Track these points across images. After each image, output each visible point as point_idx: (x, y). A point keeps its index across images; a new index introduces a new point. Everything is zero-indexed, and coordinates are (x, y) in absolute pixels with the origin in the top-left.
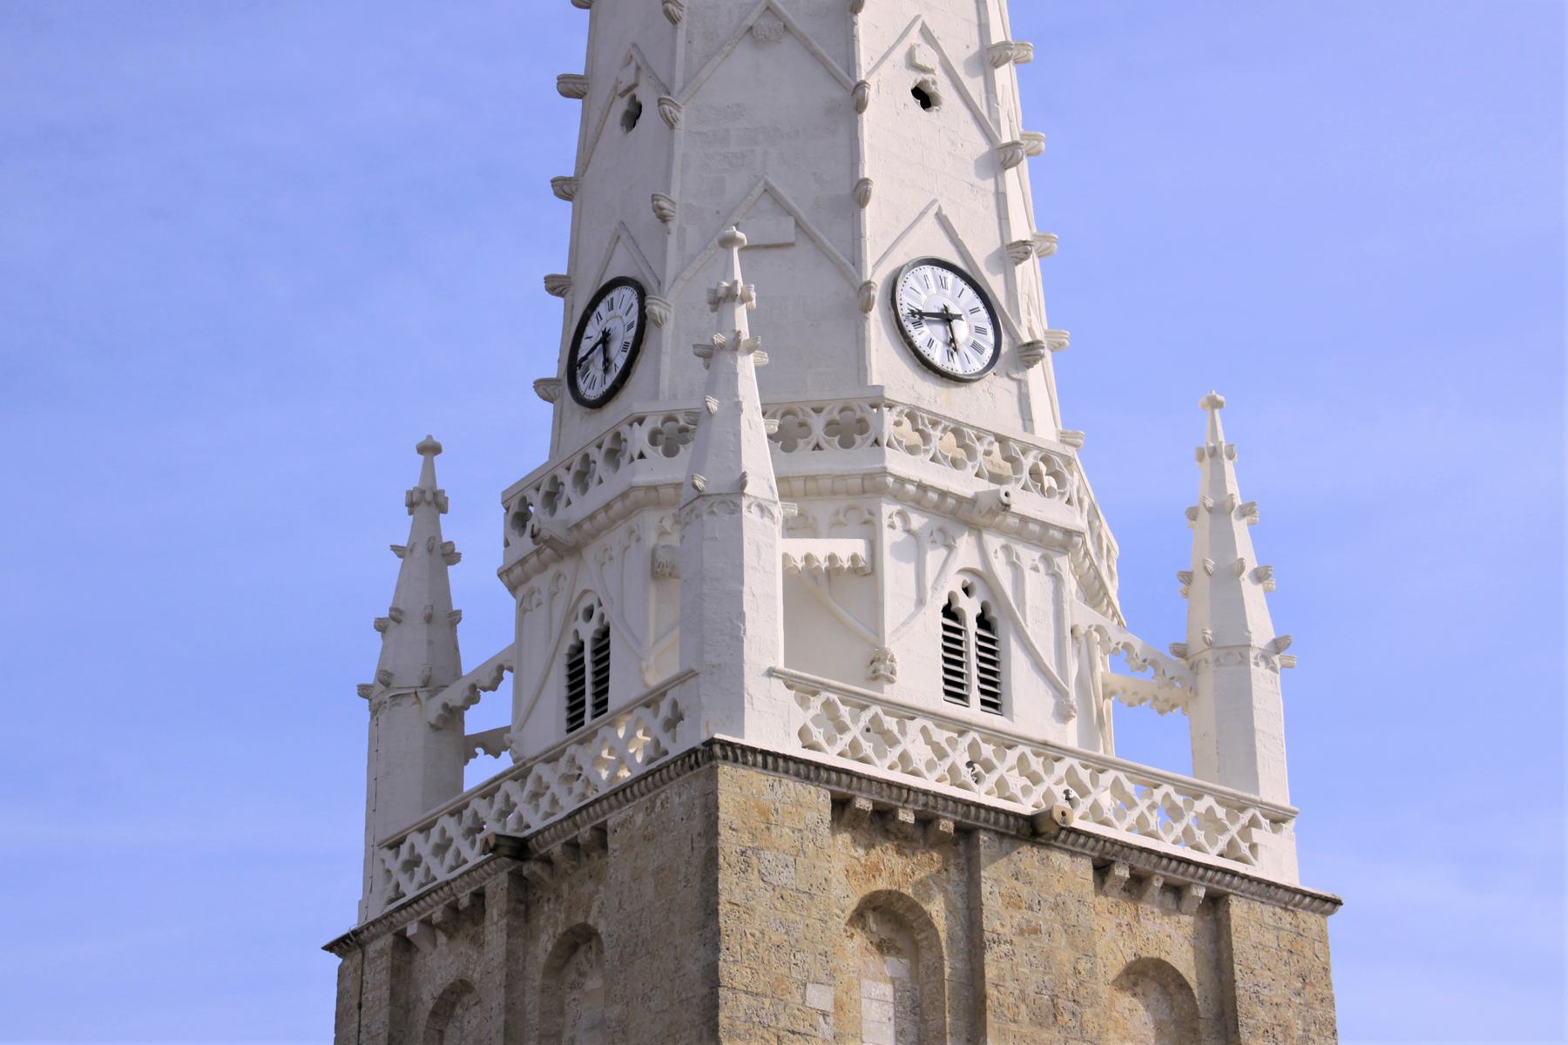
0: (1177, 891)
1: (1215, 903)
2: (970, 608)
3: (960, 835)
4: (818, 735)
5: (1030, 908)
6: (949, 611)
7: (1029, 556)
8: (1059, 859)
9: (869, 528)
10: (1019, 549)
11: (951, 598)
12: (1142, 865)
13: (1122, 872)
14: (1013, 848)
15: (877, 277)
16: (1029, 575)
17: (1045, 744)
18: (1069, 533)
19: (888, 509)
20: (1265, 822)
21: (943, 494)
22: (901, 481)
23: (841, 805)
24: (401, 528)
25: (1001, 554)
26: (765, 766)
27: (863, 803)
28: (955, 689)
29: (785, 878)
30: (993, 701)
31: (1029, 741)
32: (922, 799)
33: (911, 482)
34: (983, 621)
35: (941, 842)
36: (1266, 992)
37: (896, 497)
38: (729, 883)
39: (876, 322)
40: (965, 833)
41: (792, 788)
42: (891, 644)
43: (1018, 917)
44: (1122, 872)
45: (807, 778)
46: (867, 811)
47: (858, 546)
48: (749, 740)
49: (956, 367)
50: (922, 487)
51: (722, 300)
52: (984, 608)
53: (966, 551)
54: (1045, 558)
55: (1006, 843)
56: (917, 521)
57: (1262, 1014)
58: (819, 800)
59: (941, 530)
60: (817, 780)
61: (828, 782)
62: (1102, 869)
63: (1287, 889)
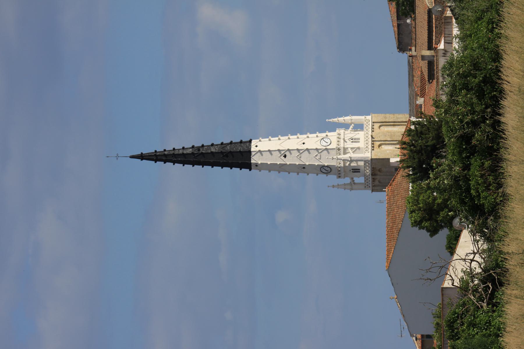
1: (373, 123)
7: (346, 136)
9: (347, 148)
15: (324, 148)
23: (373, 150)
24: (336, 189)
28: (359, 142)
38: (381, 157)
39: (328, 147)
40: (373, 141)
42: (357, 147)
47: (349, 149)
48: (370, 156)
51: (333, 159)
53: (347, 141)
62: (373, 131)
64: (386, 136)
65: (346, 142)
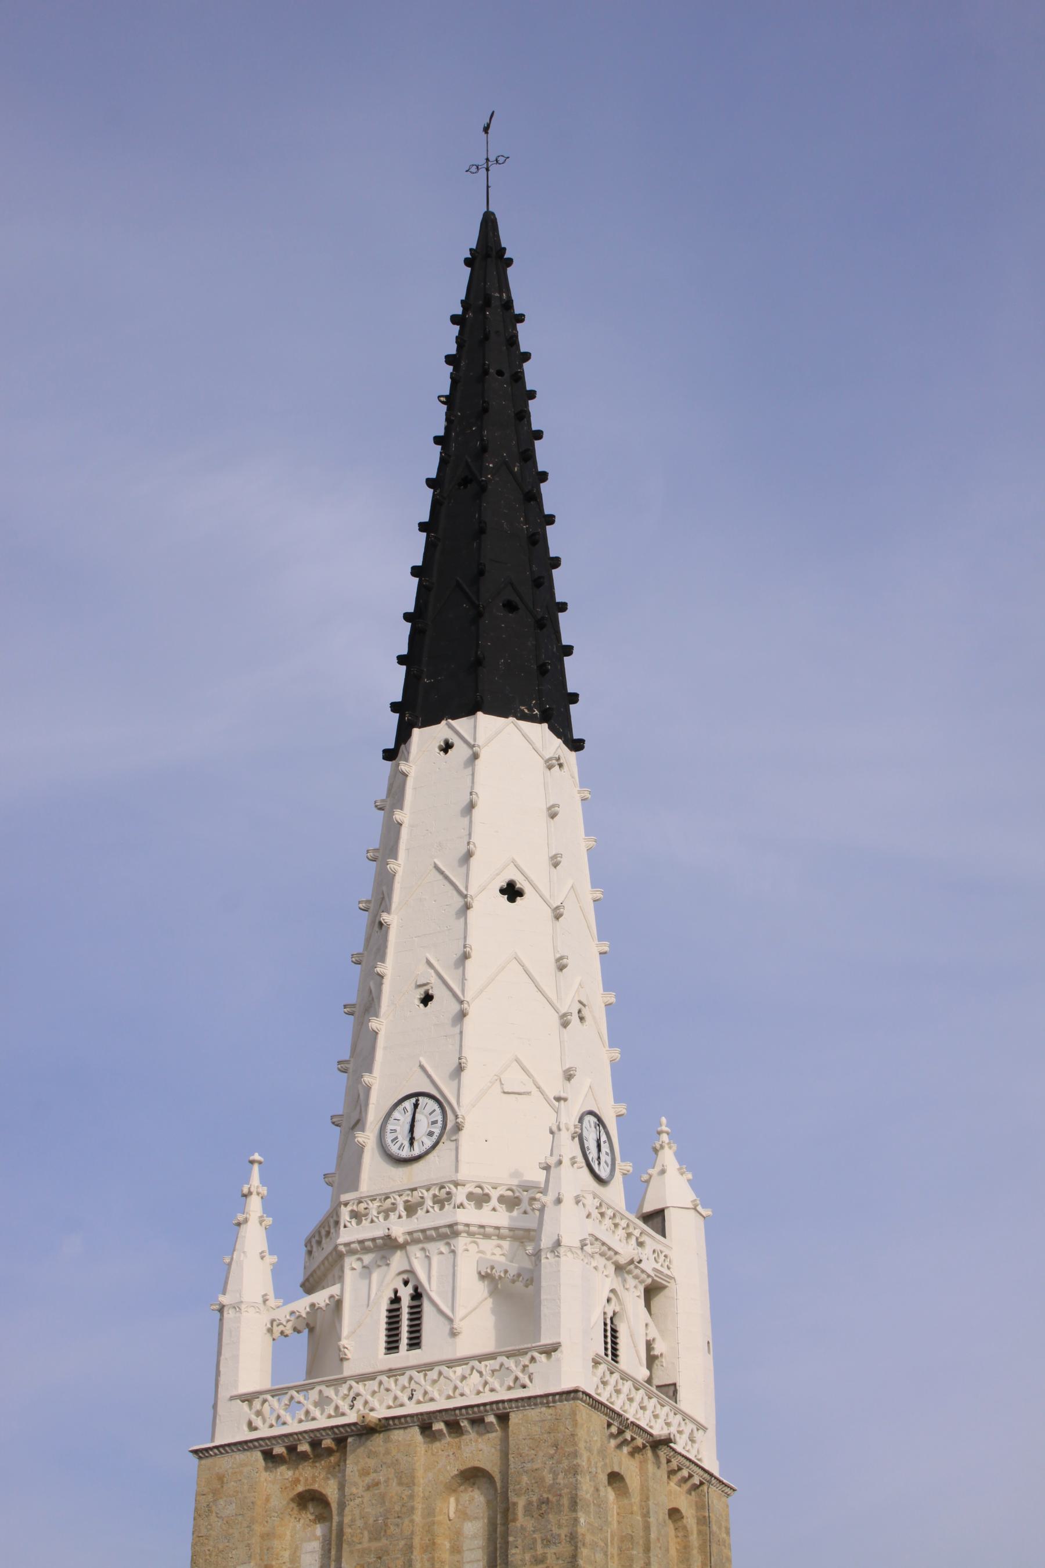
0: (477, 1422)
1: (503, 1419)
2: (405, 1294)
3: (334, 1445)
4: (258, 1422)
5: (375, 1471)
6: (396, 1300)
7: (433, 1247)
8: (397, 1435)
10: (427, 1246)
11: (396, 1292)
12: (450, 1417)
13: (439, 1426)
14: (367, 1439)
16: (435, 1259)
17: (390, 1370)
18: (450, 1226)
19: (350, 1262)
20: (543, 1358)
21: (373, 1240)
22: (347, 1245)
23: (268, 1455)
25: (420, 1254)
26: (221, 1453)
27: (279, 1450)
28: (392, 1346)
29: (231, 1510)
30: (415, 1343)
31: (382, 1372)
32: (306, 1436)
33: (353, 1242)
34: (417, 1295)
35: (329, 1451)
36: (529, 1465)
37: (352, 1252)
41: (240, 1457)
43: (368, 1480)
44: (439, 1426)
45: (245, 1450)
46: (283, 1452)
47: (334, 1290)
49: (417, 1151)
50: (361, 1242)
52: (416, 1289)
53: (398, 1262)
54: (448, 1244)
55: (363, 1439)
56: (368, 1258)
57: (525, 1479)
58: (258, 1455)
59: (384, 1258)
60: (250, 1449)
61: (255, 1447)
63: (541, 1396)
64: (378, 1532)
65: (385, 1261)
